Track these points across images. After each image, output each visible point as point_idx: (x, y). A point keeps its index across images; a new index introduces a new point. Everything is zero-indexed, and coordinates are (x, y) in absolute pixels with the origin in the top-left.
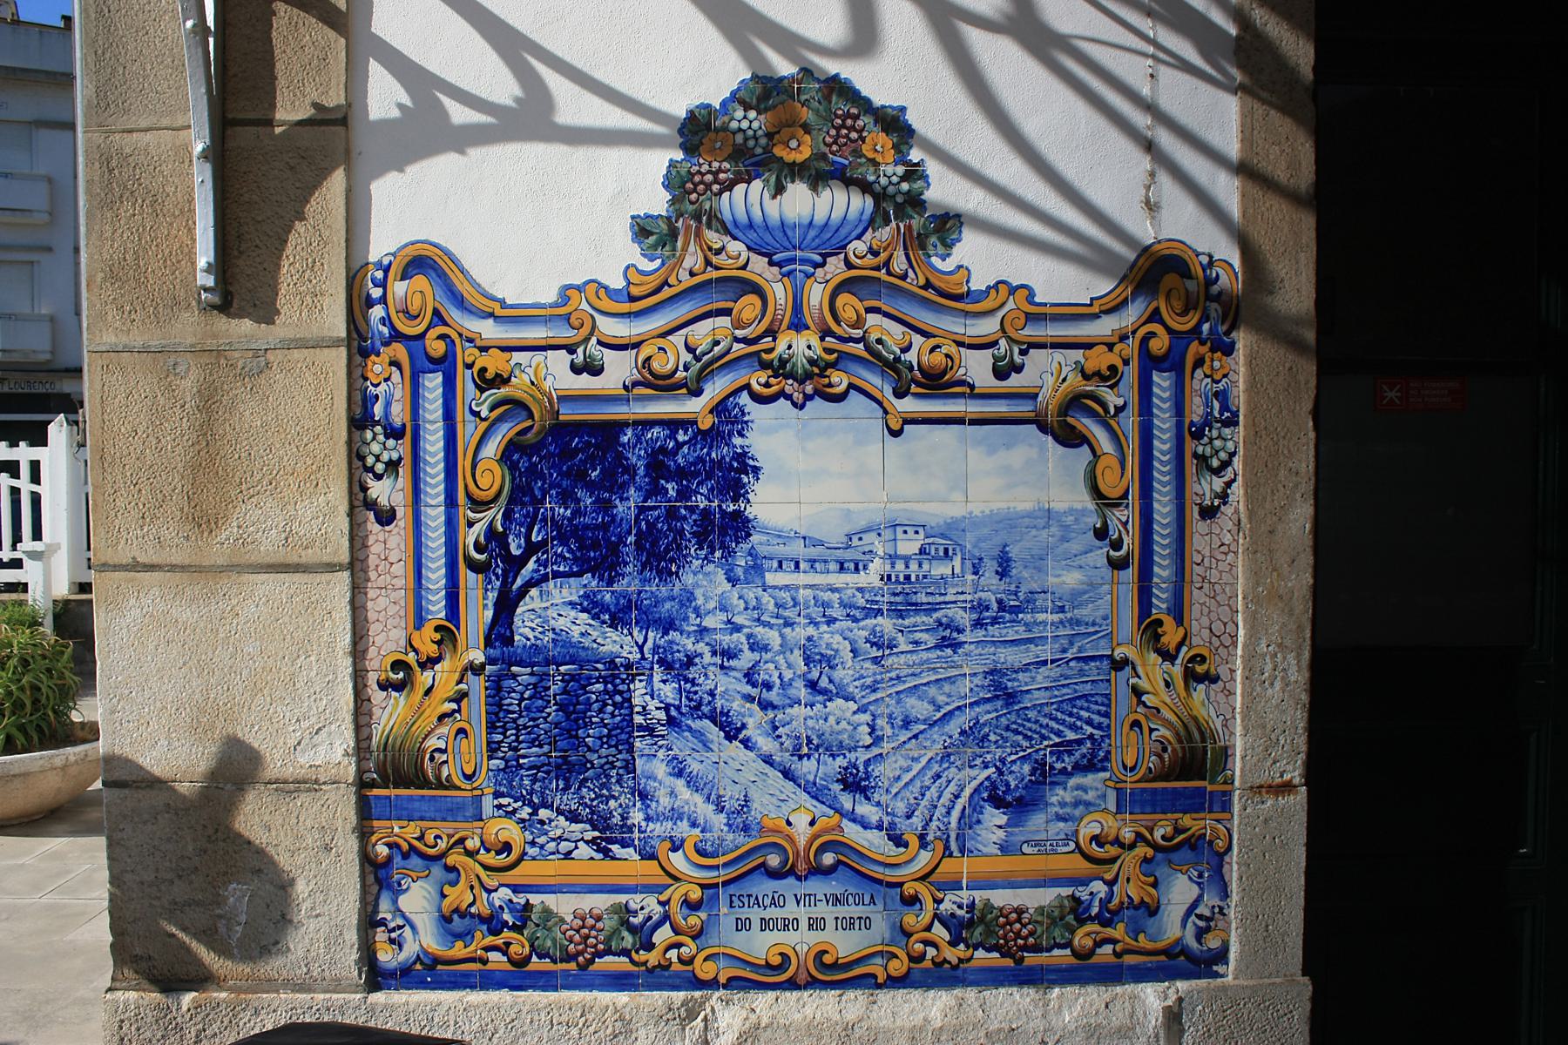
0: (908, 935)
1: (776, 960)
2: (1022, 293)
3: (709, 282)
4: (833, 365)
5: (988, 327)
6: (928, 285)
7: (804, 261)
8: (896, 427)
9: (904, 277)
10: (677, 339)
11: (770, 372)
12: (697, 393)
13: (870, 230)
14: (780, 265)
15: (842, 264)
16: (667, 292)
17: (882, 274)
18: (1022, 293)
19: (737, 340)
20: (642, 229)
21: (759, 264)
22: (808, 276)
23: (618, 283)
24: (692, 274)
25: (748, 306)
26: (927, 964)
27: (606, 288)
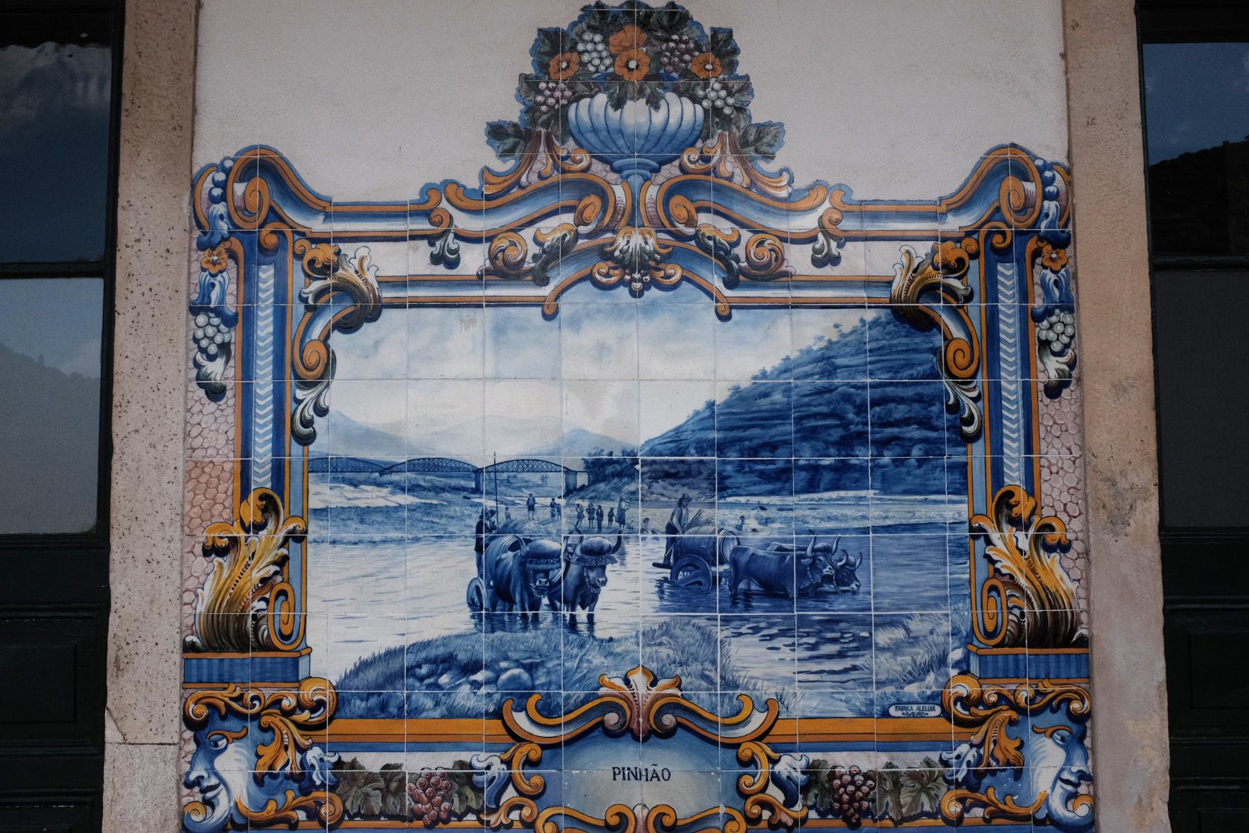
0: (745, 796)
4: (667, 258)
5: (807, 223)
9: (730, 179)
10: (528, 234)
11: (610, 264)
12: (544, 282)
13: (700, 141)
14: (618, 171)
15: (678, 172)
16: (515, 192)
21: (598, 167)
22: (647, 179)
23: (473, 182)
24: (541, 177)
26: (763, 824)
27: (464, 187)
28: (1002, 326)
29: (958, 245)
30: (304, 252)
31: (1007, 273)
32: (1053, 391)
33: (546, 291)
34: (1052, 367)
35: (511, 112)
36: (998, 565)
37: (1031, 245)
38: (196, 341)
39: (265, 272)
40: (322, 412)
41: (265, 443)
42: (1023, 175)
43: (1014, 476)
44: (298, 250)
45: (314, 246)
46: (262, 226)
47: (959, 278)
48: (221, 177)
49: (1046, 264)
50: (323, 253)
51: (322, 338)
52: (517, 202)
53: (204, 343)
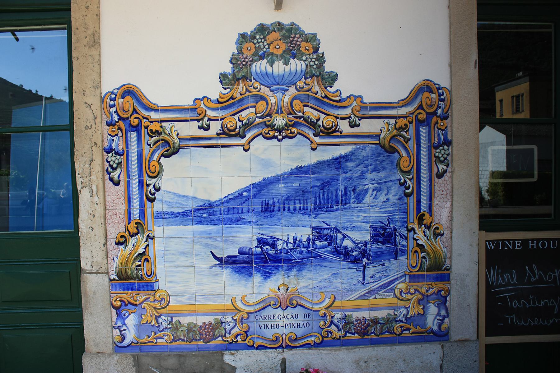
1: (274, 339)
2: (359, 100)
3: (248, 97)
6: (326, 97)
7: (281, 89)
8: (314, 146)
10: (236, 117)
11: (269, 129)
12: (243, 137)
17: (309, 93)
18: (359, 100)
19: (257, 117)
20: (223, 77)
24: (241, 95)
25: (262, 105)
28: (422, 152)
29: (405, 119)
30: (148, 126)
31: (423, 130)
32: (440, 176)
33: (243, 141)
34: (441, 167)
35: (228, 68)
36: (418, 242)
37: (434, 119)
38: (108, 162)
39: (133, 134)
40: (158, 190)
41: (137, 202)
42: (431, 92)
43: (424, 208)
44: (146, 125)
45: (151, 124)
46: (131, 115)
47: (406, 132)
48: (113, 96)
49: (439, 127)
50: (155, 127)
51: (158, 161)
52: (233, 104)
53: (111, 163)
